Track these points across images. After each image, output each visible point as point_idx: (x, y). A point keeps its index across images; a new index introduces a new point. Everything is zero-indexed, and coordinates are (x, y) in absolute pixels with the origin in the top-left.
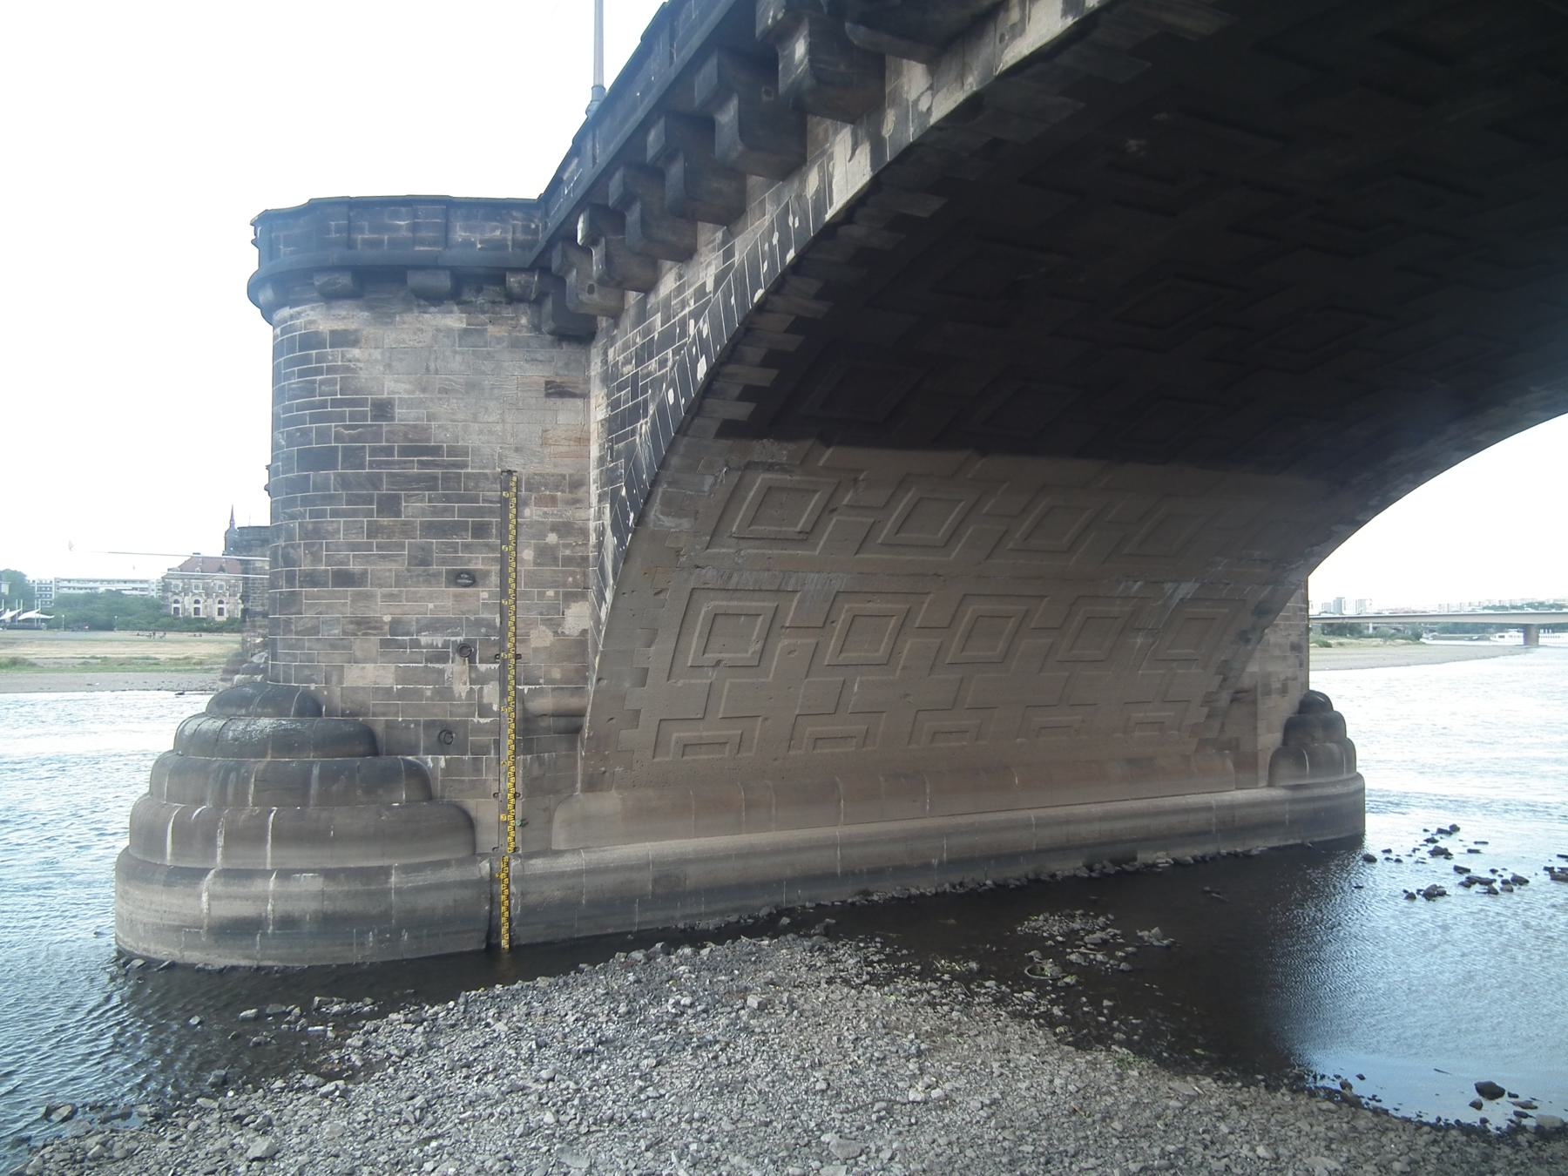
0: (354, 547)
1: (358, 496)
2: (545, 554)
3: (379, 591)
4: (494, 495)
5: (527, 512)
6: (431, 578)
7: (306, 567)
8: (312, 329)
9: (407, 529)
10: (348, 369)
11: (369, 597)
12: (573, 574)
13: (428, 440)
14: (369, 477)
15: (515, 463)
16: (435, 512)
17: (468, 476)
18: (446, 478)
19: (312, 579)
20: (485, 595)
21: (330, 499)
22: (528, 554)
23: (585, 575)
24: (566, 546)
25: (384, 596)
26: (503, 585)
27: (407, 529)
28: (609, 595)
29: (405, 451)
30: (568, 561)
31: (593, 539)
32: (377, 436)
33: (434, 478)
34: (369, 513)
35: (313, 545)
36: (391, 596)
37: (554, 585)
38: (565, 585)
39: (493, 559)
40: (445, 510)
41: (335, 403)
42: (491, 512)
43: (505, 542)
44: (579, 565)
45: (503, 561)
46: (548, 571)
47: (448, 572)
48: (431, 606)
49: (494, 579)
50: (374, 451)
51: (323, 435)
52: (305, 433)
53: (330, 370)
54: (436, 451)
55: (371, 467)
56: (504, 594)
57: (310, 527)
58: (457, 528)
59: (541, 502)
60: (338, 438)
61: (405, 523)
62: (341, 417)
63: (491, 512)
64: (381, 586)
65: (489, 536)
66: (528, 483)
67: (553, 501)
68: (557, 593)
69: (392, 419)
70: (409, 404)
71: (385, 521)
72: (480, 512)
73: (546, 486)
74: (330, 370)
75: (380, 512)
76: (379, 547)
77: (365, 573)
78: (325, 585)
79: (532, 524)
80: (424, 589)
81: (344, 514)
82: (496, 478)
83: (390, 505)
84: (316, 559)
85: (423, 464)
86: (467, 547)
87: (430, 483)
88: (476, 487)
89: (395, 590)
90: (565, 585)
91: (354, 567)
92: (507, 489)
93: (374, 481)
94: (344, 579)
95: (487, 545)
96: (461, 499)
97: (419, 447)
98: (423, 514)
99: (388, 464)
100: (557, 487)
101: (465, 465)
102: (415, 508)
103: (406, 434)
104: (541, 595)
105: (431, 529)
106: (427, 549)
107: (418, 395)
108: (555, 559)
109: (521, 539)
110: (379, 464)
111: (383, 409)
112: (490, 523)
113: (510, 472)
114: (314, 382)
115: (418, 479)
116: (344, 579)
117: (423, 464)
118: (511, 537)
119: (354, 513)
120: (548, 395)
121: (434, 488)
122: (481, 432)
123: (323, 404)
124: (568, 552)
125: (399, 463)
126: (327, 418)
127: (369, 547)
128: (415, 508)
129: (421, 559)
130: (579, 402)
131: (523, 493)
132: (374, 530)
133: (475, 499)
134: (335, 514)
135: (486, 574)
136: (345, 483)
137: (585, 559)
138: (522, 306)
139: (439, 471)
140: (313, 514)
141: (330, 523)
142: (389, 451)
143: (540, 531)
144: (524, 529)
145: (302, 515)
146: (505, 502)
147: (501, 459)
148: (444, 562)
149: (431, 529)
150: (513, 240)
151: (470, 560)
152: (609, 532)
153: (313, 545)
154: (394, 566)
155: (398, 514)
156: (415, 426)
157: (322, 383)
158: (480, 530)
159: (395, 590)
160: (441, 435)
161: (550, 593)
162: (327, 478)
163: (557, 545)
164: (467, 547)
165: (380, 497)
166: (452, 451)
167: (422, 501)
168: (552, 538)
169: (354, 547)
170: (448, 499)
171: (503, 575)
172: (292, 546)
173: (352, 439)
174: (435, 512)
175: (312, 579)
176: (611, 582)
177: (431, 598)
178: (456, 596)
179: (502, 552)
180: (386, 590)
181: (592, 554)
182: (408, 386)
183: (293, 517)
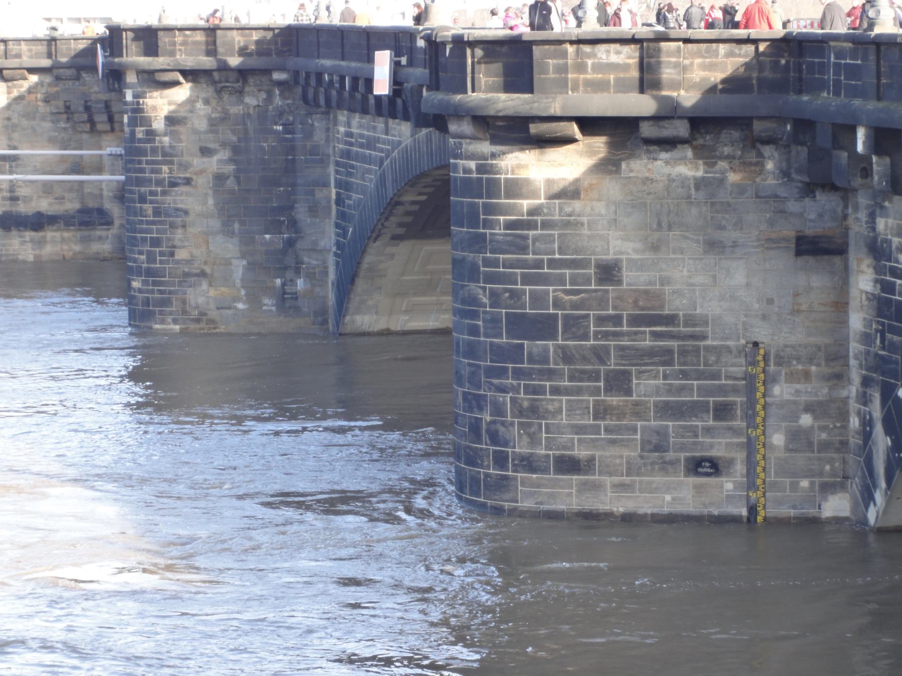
0: (579, 430)
1: (583, 372)
2: (799, 439)
3: (608, 480)
4: (738, 371)
5: (777, 390)
6: (666, 466)
7: (522, 448)
8: (522, 174)
9: (638, 410)
10: (567, 224)
11: (597, 487)
12: (831, 461)
13: (662, 307)
14: (594, 349)
15: (762, 333)
16: (670, 390)
17: (707, 349)
18: (683, 352)
19: (529, 464)
20: (729, 486)
21: (550, 374)
22: (778, 439)
23: (844, 461)
24: (823, 428)
25: (615, 486)
26: (751, 472)
27: (638, 410)
28: (879, 496)
29: (636, 320)
30: (825, 446)
31: (854, 422)
32: (602, 303)
33: (669, 352)
34: (596, 392)
35: (529, 425)
36: (621, 487)
37: (809, 474)
38: (821, 474)
39: (739, 445)
40: (681, 389)
41: (552, 263)
42: (735, 390)
43: (751, 424)
44: (838, 450)
45: (750, 447)
46: (801, 459)
47: (687, 460)
48: (668, 498)
49: (740, 468)
50: (601, 320)
51: (538, 299)
52: (514, 294)
53: (546, 225)
54: (671, 320)
55: (596, 339)
56: (751, 485)
57: (526, 404)
58: (696, 409)
59: (792, 377)
60: (557, 304)
61: (637, 404)
62: (561, 280)
63: (735, 390)
64: (610, 474)
65: (733, 418)
66: (777, 356)
67: (807, 375)
68: (812, 484)
69: (619, 282)
70: (641, 266)
71: (614, 400)
72: (722, 390)
73: (798, 359)
74: (546, 225)
75: (609, 390)
76: (608, 430)
77: (591, 459)
78: (546, 471)
79: (782, 405)
80: (658, 479)
81: (567, 392)
82: (741, 351)
83: (619, 382)
84: (534, 440)
85: (656, 335)
86: (708, 431)
87: (666, 357)
88: (718, 361)
89: (626, 479)
90: (821, 474)
91: (580, 453)
92: (754, 364)
93: (600, 355)
94: (569, 465)
95: (730, 428)
96: (700, 376)
97: (652, 317)
98: (658, 393)
99: (616, 335)
100: (811, 360)
101: (704, 338)
102: (648, 386)
103: (636, 302)
104: (794, 486)
105: (668, 410)
106: (662, 433)
107: (647, 255)
108: (810, 444)
109: (771, 421)
110: (606, 335)
111: (608, 272)
112: (734, 403)
113: (756, 344)
114: (525, 238)
115: (651, 353)
116: (569, 465)
117: (656, 335)
118: (759, 420)
119: (579, 391)
120: (799, 253)
121: (669, 363)
122: (722, 298)
123: (538, 264)
124: (824, 436)
125: (628, 334)
126: (544, 280)
127: (596, 430)
128: (648, 386)
129: (657, 445)
130: (837, 260)
131: (772, 368)
132: (601, 411)
133: (715, 376)
134: (556, 391)
135: (731, 462)
136: (566, 356)
137: (844, 444)
138: (767, 150)
139: (674, 344)
140: (529, 390)
141: (550, 402)
142: (616, 320)
143: (792, 410)
144: (773, 410)
145: (516, 390)
146: (750, 379)
147: (746, 329)
148: (682, 448)
149: (668, 410)
150: (759, 80)
151: (712, 446)
152: (879, 429)
153: (529, 425)
154: (626, 453)
155: (629, 392)
156: (646, 292)
157: (536, 239)
158: (723, 411)
159: (626, 479)
160: (676, 305)
161: (805, 483)
162: (546, 349)
163: (812, 427)
164: (708, 431)
165: (608, 373)
166: (690, 320)
167: (656, 377)
168: (806, 420)
169: (579, 430)
170: (685, 375)
171: (751, 464)
172: (503, 423)
173: (575, 306)
174: (670, 390)
175: (529, 464)
176: (883, 485)
177: (668, 490)
178: (698, 488)
179: (749, 438)
180: (616, 479)
181: (855, 441)
182: (638, 245)
183: (503, 390)
